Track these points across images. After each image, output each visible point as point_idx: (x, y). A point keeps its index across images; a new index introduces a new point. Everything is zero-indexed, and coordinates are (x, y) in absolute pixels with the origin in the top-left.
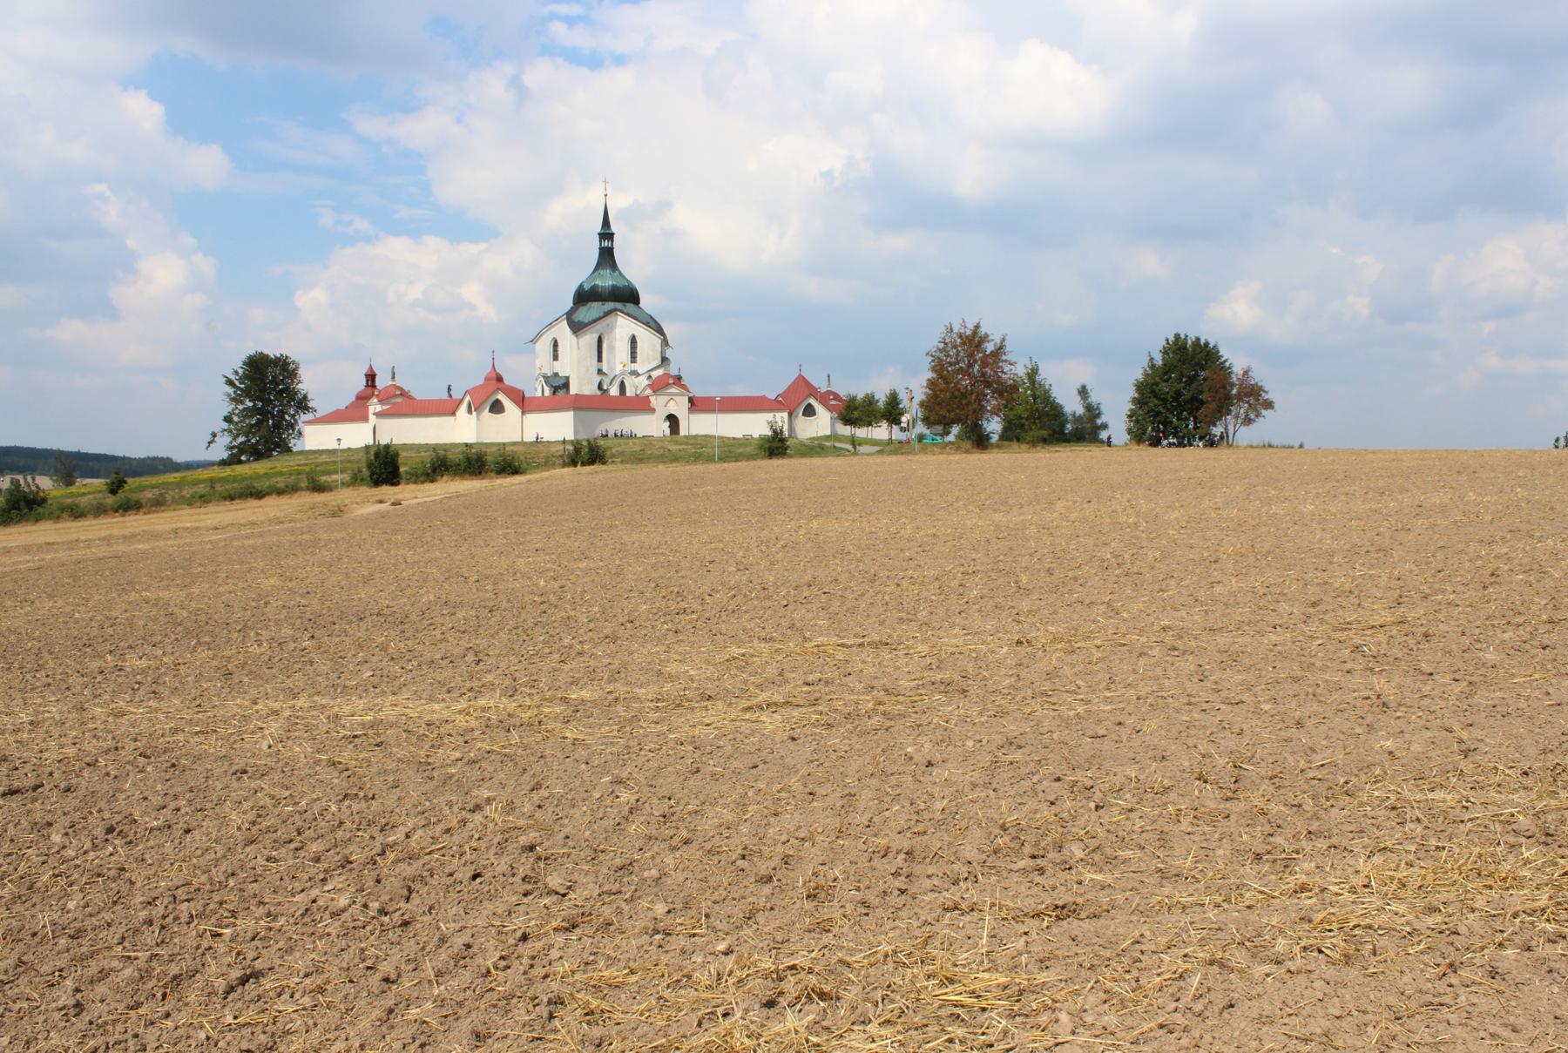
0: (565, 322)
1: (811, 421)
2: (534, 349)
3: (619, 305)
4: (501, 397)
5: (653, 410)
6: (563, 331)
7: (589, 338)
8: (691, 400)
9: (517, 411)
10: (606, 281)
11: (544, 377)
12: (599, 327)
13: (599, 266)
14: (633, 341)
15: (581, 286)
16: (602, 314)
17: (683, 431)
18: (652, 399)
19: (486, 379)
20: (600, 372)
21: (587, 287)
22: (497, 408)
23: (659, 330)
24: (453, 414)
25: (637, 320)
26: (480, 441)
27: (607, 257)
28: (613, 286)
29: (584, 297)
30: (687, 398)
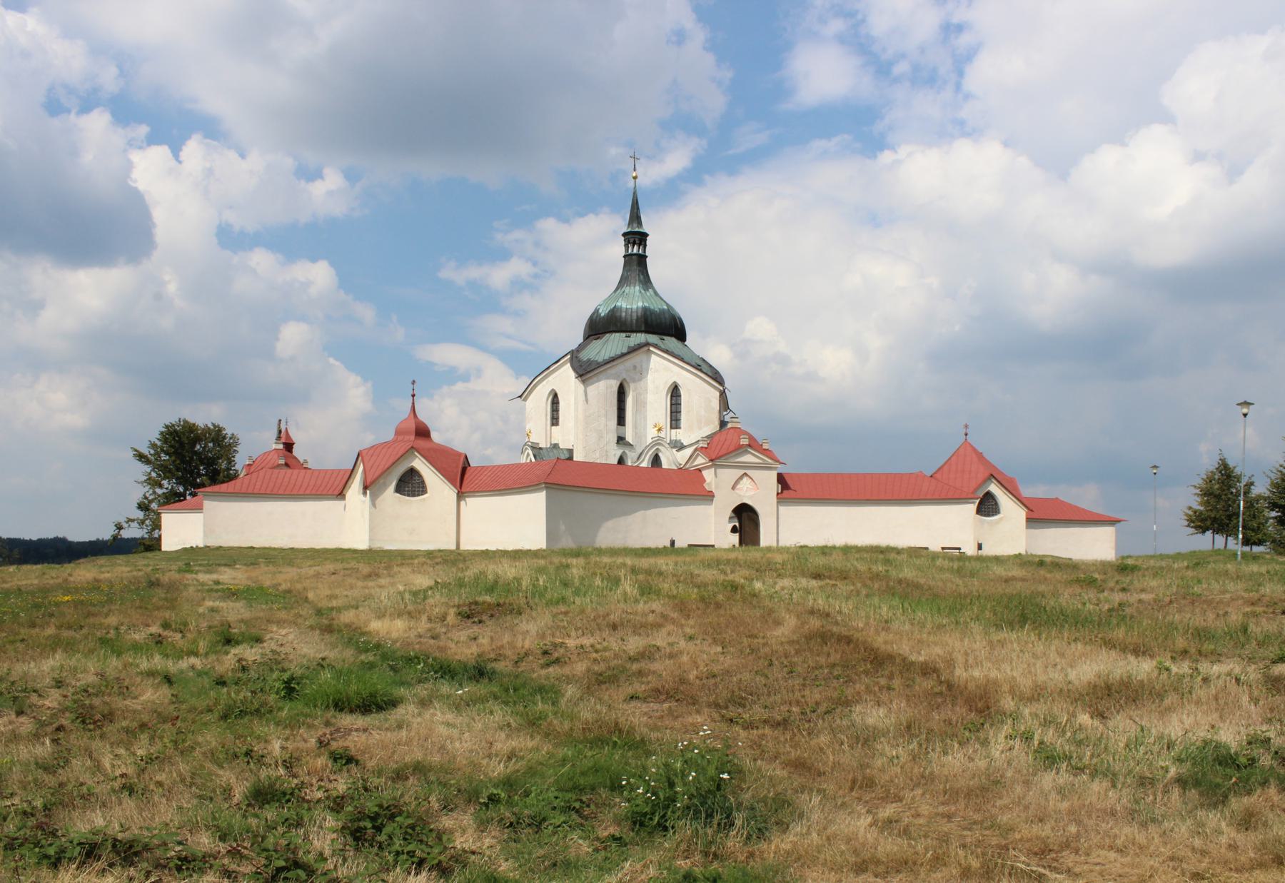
0: (569, 365)
1: (998, 522)
2: (524, 408)
3: (653, 338)
4: (420, 464)
5: (708, 497)
6: (565, 380)
7: (604, 388)
8: (781, 479)
9: (449, 492)
10: (633, 301)
11: (533, 448)
12: (621, 368)
13: (624, 281)
14: (675, 392)
15: (597, 311)
16: (625, 350)
17: (767, 538)
18: (708, 475)
19: (398, 432)
20: (621, 440)
21: (603, 312)
22: (410, 484)
23: (721, 382)
24: (341, 495)
25: (682, 360)
26: (213, 543)
27: (636, 265)
28: (645, 310)
29: (598, 327)
30: (773, 475)
